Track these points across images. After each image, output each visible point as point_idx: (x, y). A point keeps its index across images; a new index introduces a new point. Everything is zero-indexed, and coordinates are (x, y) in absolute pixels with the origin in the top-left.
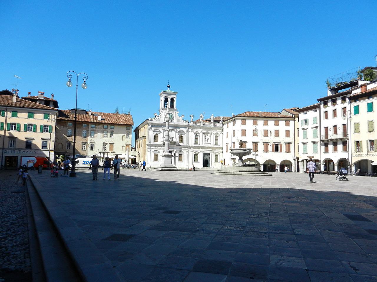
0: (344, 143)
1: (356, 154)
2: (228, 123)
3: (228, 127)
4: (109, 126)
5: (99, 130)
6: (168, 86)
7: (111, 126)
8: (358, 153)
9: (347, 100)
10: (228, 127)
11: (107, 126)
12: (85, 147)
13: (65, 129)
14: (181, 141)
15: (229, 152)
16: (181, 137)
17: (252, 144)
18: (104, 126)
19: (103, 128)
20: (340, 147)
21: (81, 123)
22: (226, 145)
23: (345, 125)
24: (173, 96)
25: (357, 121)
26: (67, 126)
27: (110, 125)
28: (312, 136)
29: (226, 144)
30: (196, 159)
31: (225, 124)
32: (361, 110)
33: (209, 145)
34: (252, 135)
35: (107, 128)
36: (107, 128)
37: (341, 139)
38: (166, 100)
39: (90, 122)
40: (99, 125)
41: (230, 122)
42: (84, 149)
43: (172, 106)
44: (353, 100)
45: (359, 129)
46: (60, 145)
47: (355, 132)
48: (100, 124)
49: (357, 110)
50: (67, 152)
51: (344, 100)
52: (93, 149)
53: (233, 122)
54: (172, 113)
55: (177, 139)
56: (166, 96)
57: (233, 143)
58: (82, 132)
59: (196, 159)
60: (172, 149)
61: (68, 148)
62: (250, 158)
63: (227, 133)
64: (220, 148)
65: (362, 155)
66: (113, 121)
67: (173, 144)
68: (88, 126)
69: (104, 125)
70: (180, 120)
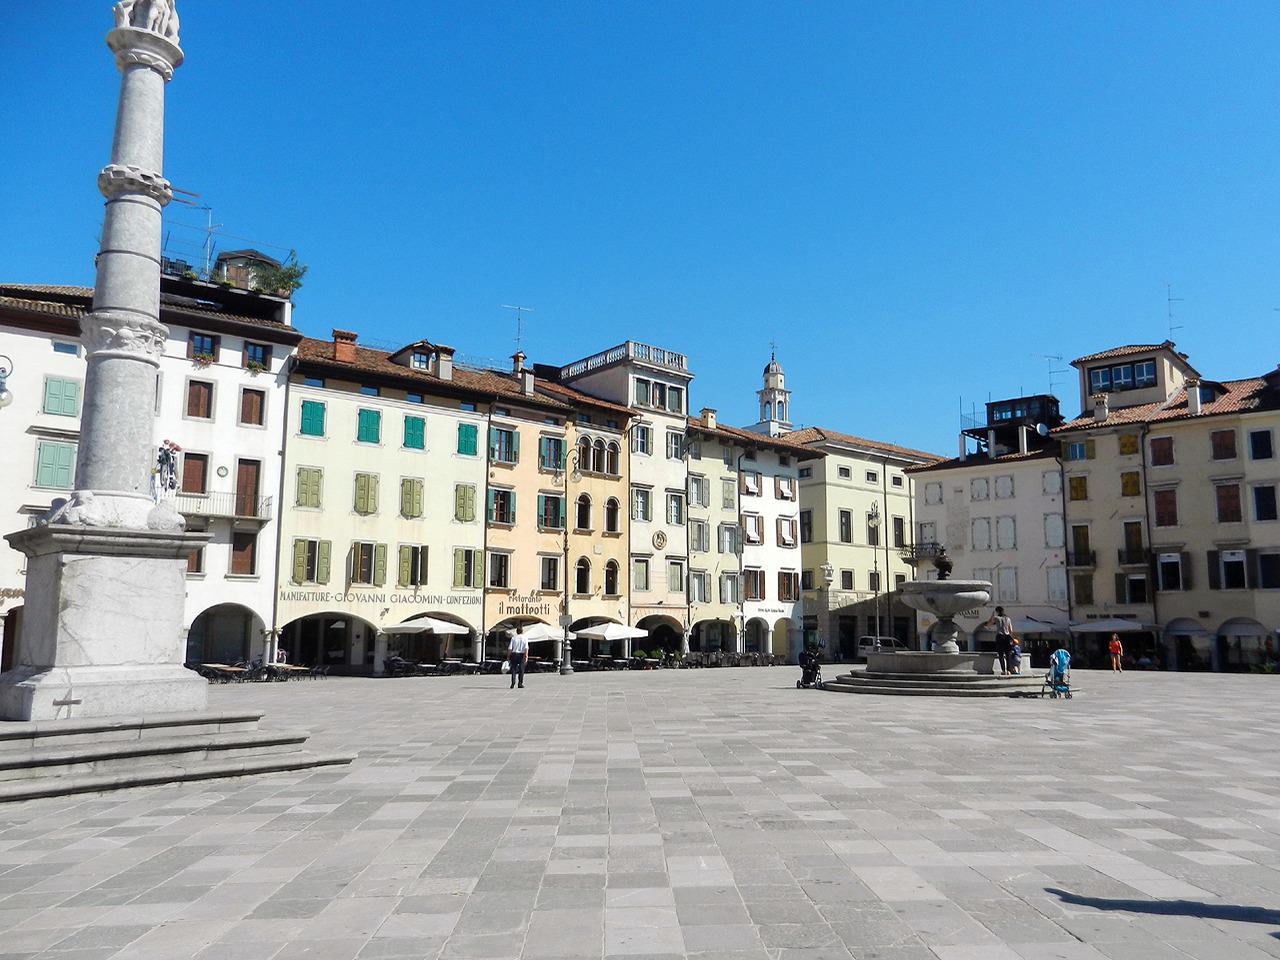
0: (244, 543)
1: (296, 589)
8: (309, 587)
9: (277, 364)
20: (218, 554)
23: (250, 470)
25: (309, 462)
28: (29, 476)
32: (330, 421)
37: (229, 520)
44: (303, 377)
45: (317, 494)
47: (299, 503)
49: (313, 421)
51: (257, 361)
65: (323, 597)
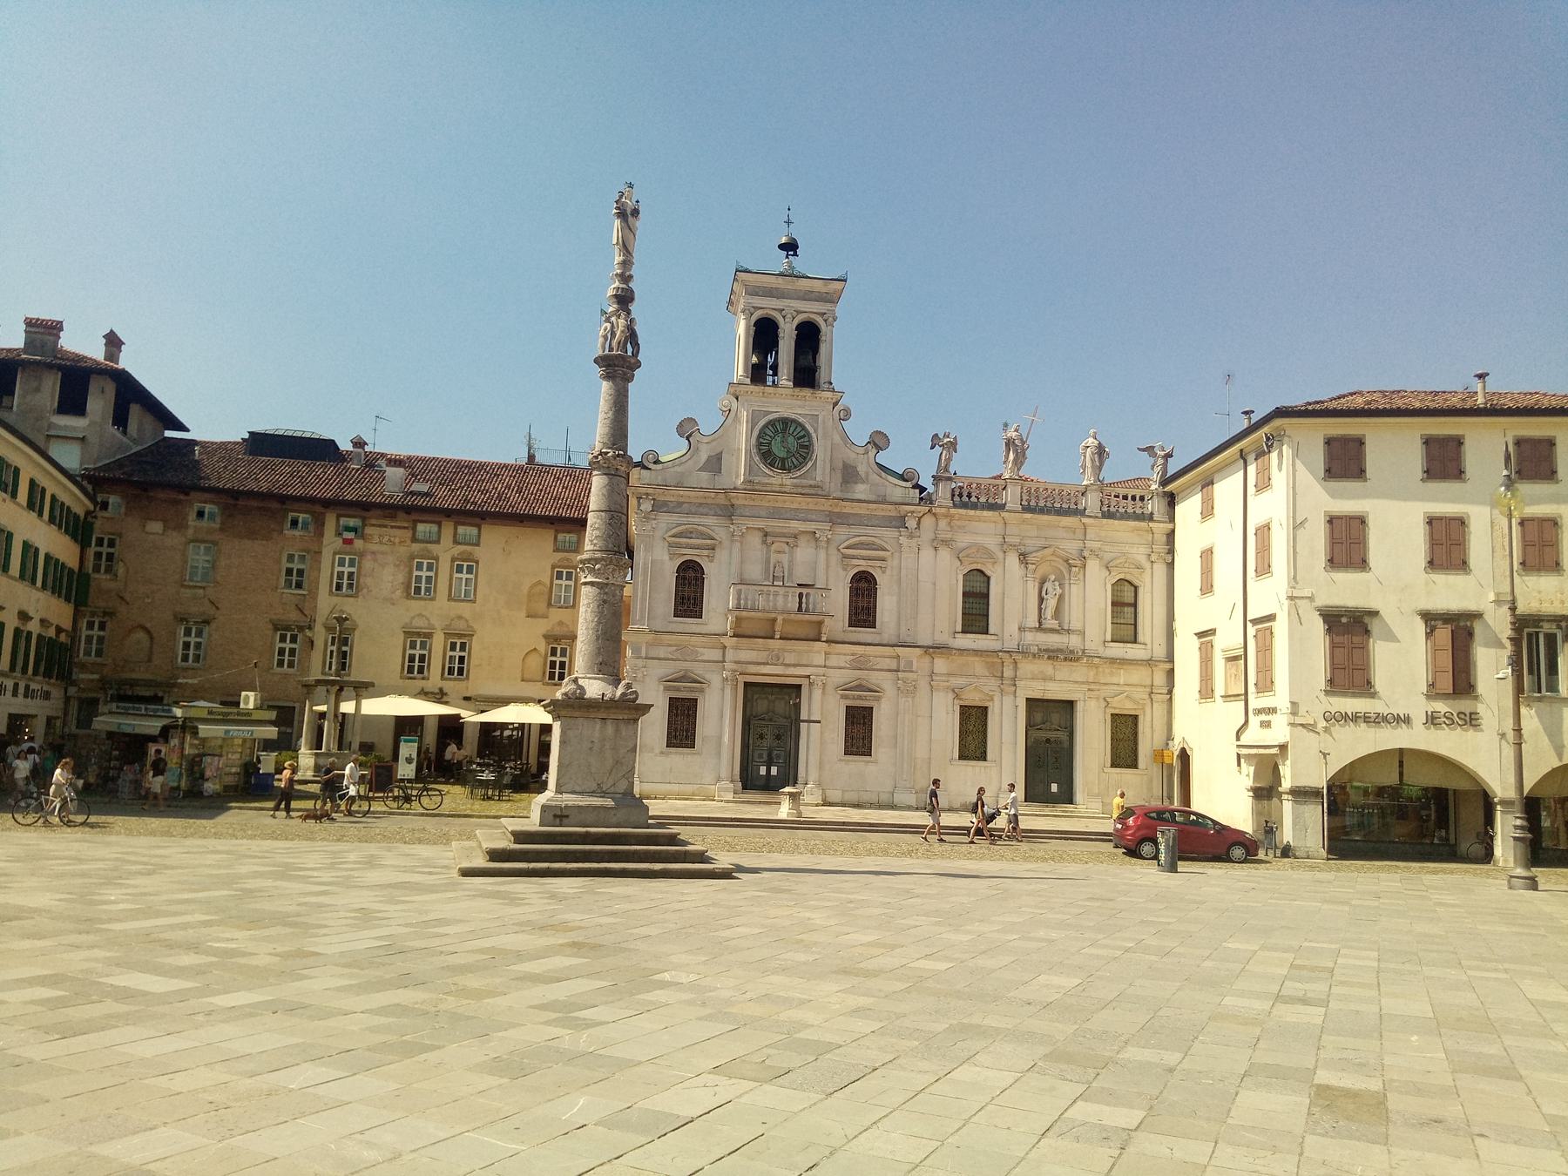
2: (1212, 483)
3: (1208, 511)
4: (448, 529)
5: (383, 553)
6: (784, 240)
7: (461, 529)
10: (1208, 511)
11: (434, 528)
12: (292, 652)
13: (174, 539)
14: (863, 608)
15: (1219, 690)
16: (864, 589)
17: (1420, 627)
18: (421, 527)
19: (414, 540)
21: (275, 505)
22: (1196, 642)
24: (811, 310)
26: (181, 526)
27: (457, 524)
29: (1200, 635)
30: (973, 743)
31: (1188, 491)
33: (1074, 642)
34: (1423, 563)
35: (438, 542)
36: (438, 542)
38: (764, 334)
39: (328, 504)
40: (387, 522)
41: (1224, 469)
42: (291, 665)
43: (806, 376)
46: (141, 635)
48: (393, 517)
50: (174, 685)
52: (461, 671)
53: (1252, 469)
54: (801, 420)
55: (838, 601)
56: (768, 306)
57: (1255, 622)
58: (279, 562)
59: (973, 743)
60: (795, 666)
61: (185, 658)
62: (1401, 750)
63: (1207, 555)
64: (1150, 663)
66: (479, 498)
67: (801, 632)
68: (320, 524)
69: (415, 522)
70: (862, 469)
